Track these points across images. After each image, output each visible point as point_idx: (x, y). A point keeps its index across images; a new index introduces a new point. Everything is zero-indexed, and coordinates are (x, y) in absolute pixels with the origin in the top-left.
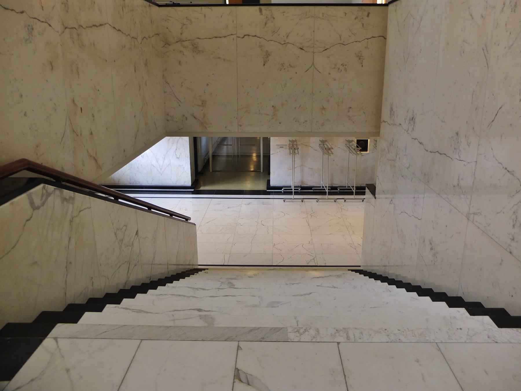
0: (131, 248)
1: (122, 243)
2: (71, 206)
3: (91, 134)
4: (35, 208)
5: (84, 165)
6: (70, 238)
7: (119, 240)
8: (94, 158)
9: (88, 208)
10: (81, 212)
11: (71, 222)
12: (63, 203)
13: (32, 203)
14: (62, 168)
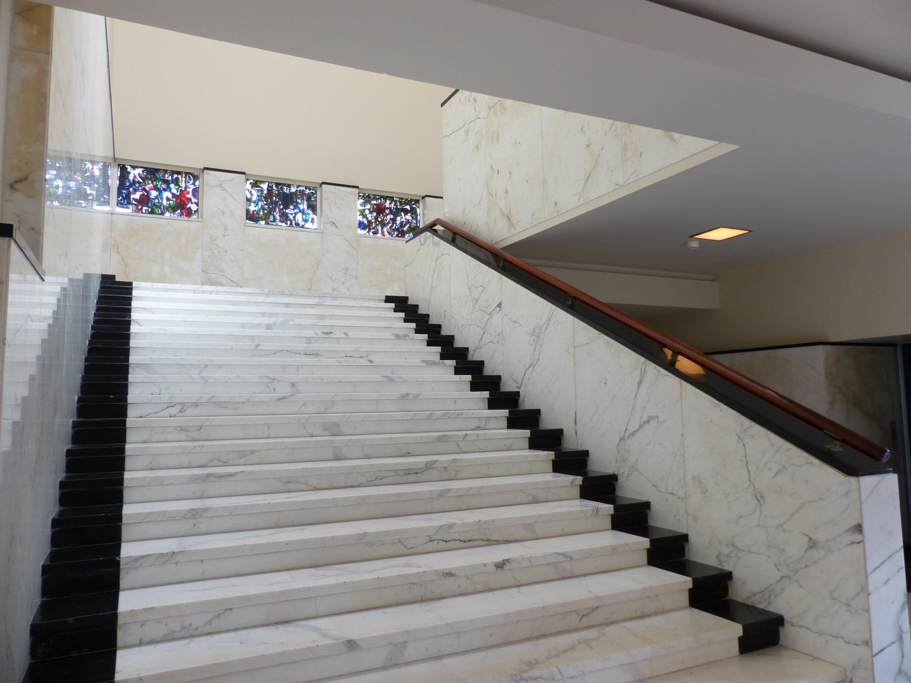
0: (487, 317)
1: (476, 303)
2: (437, 249)
3: (507, 192)
4: (422, 245)
5: (495, 223)
6: (434, 271)
7: (473, 298)
8: (508, 217)
9: (448, 254)
10: (443, 256)
11: (436, 260)
12: (433, 245)
13: (420, 241)
14: (478, 226)
